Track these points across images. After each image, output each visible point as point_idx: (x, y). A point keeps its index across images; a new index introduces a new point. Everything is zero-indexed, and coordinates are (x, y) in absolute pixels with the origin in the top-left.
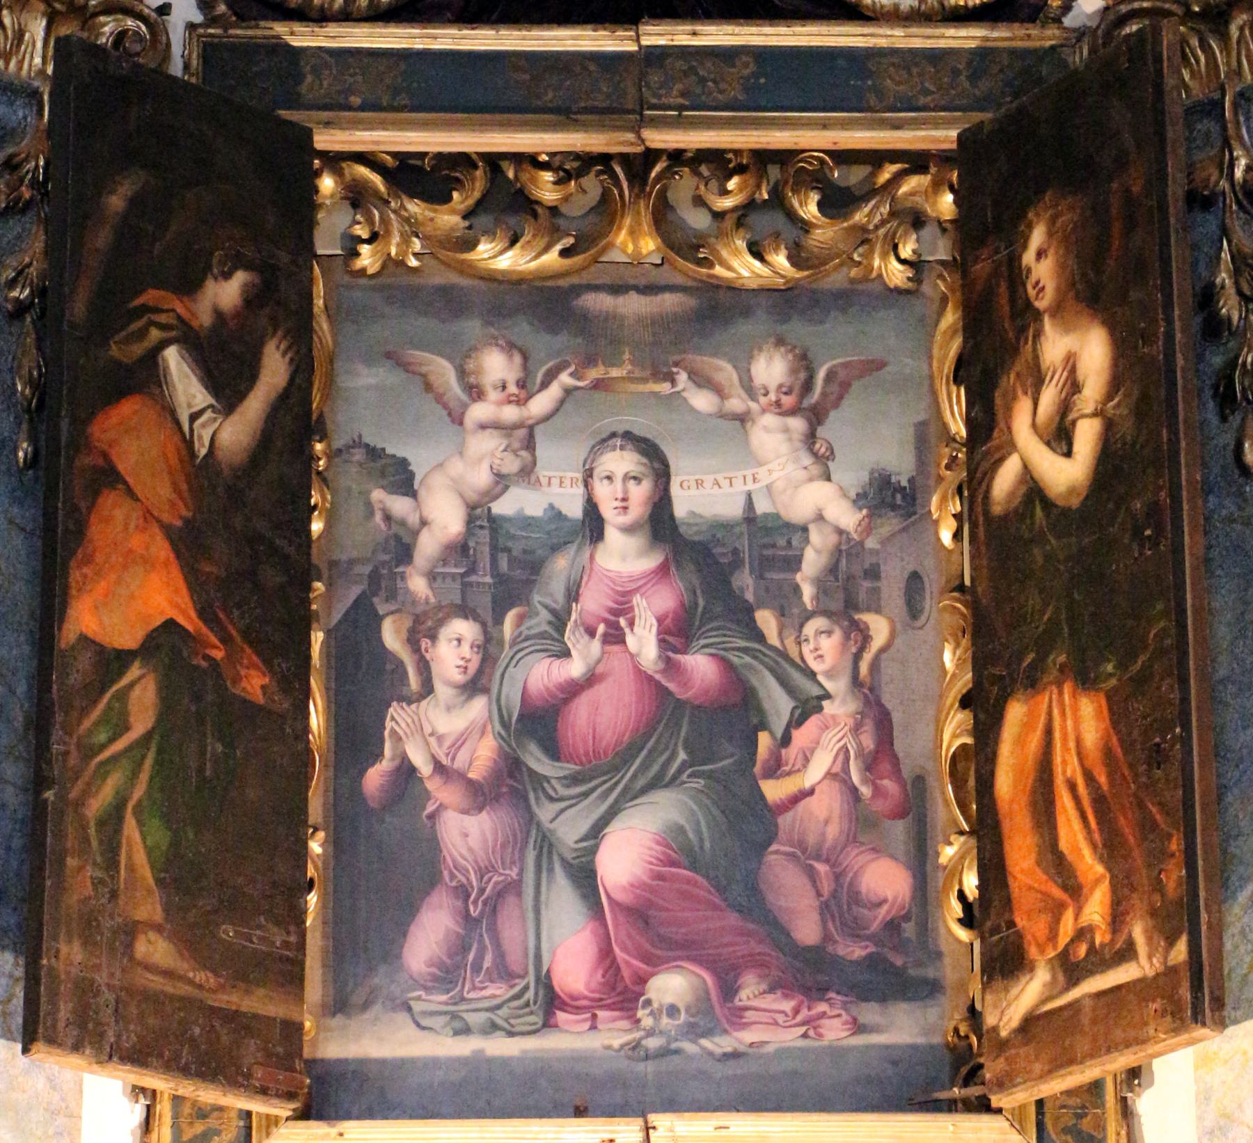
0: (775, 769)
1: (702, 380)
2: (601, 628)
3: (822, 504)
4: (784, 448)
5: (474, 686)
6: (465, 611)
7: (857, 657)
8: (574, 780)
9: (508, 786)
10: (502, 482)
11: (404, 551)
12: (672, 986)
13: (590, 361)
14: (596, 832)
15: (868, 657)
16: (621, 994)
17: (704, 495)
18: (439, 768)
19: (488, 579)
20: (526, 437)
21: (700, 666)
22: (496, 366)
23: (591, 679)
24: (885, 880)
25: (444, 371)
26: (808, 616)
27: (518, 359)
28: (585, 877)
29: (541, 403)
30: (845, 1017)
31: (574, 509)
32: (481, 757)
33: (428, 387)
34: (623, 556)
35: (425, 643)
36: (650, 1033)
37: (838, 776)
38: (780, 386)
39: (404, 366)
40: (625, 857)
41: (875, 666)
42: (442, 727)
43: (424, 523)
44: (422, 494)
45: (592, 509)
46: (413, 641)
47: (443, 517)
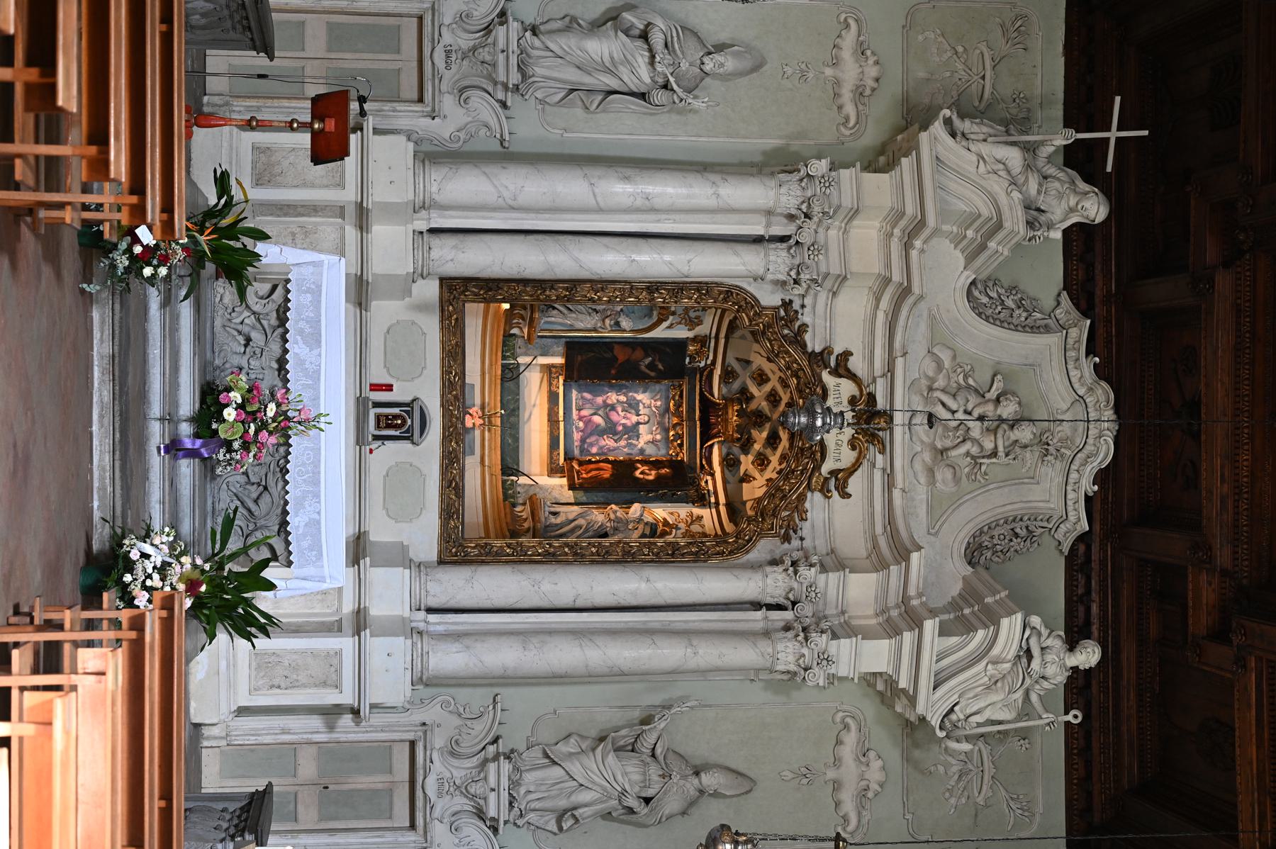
3: (641, 443)
9: (605, 405)
12: (581, 424)
16: (580, 418)
17: (642, 429)
20: (649, 407)
22: (659, 403)
24: (594, 450)
32: (609, 402)
34: (635, 419)
40: (598, 419)
42: (613, 397)
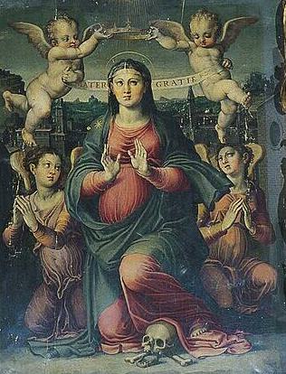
0: (207, 220)
1: (165, 32)
2: (119, 157)
4: (208, 64)
5: (55, 188)
6: (50, 150)
7: (247, 166)
8: (106, 231)
9: (74, 236)
10: (68, 86)
11: (20, 121)
13: (109, 26)
14: (119, 257)
15: (252, 165)
17: (168, 88)
18: (41, 227)
19: (63, 134)
20: (79, 64)
21: (168, 172)
22: (63, 28)
23: (114, 182)
25: (37, 32)
26: (223, 146)
27: (74, 24)
28: (113, 276)
29: (86, 47)
30: (246, 342)
31: (104, 99)
33: (30, 41)
34: (128, 121)
35: (32, 166)
36: (149, 353)
37: (239, 225)
38: (205, 33)
39: (18, 31)
40: (133, 267)
41: (256, 168)
42: (40, 207)
43: (30, 107)
44: (28, 92)
45: (112, 97)
46: (27, 168)
47: (39, 104)
